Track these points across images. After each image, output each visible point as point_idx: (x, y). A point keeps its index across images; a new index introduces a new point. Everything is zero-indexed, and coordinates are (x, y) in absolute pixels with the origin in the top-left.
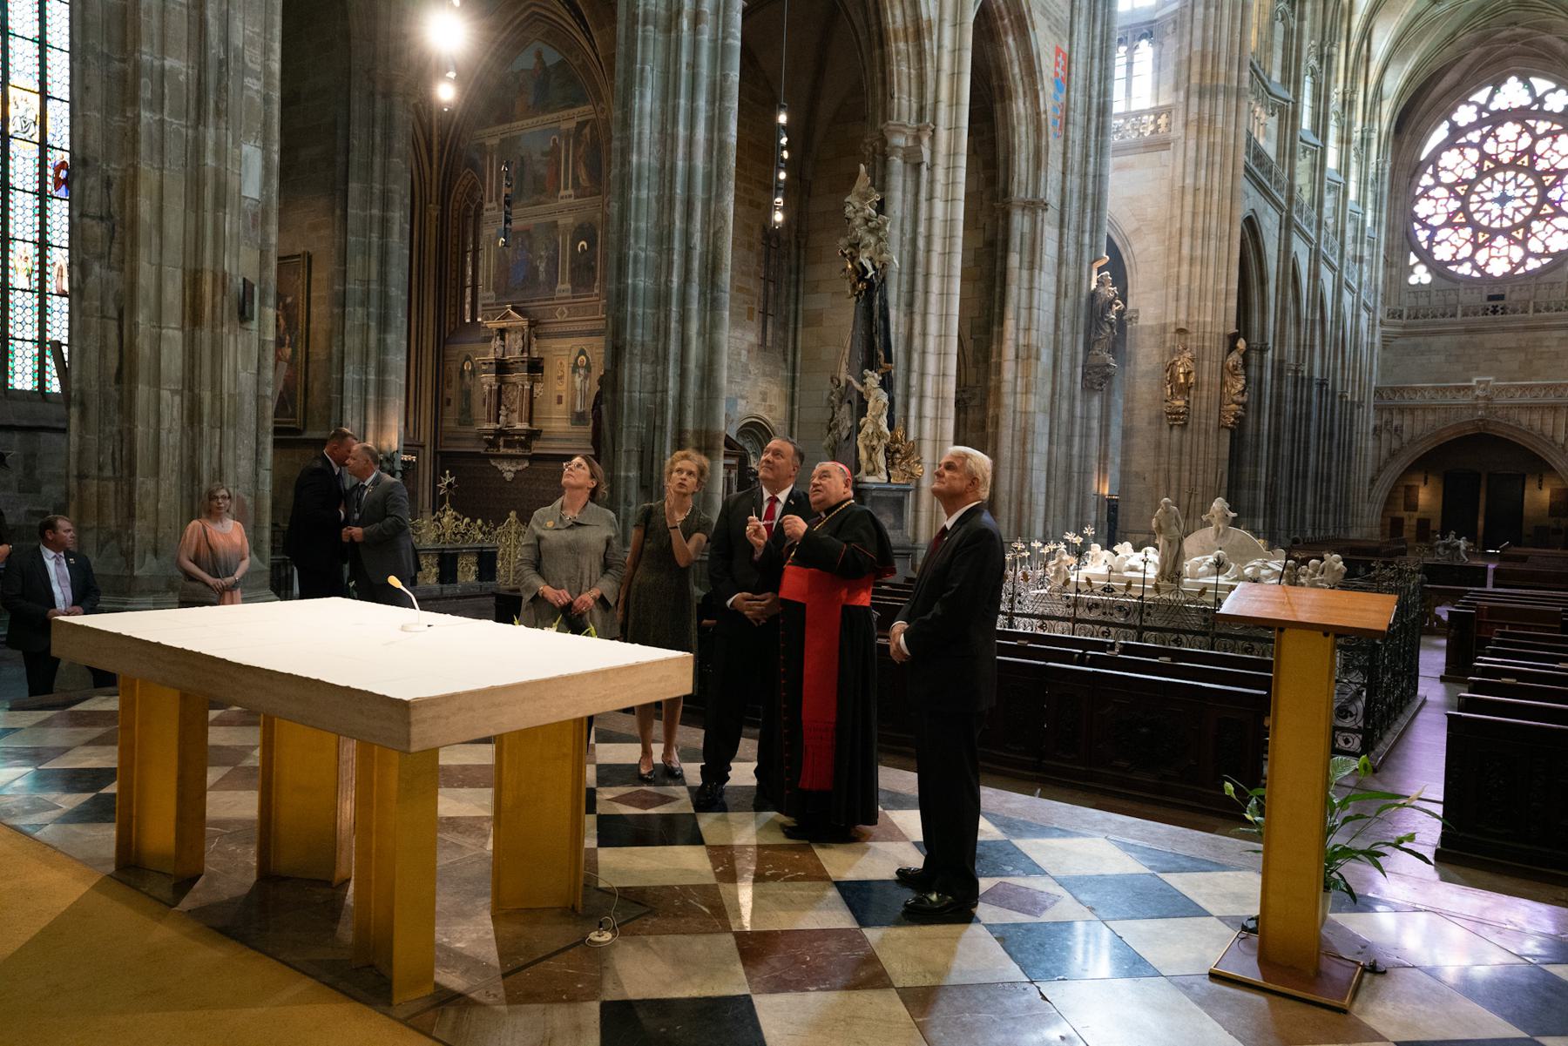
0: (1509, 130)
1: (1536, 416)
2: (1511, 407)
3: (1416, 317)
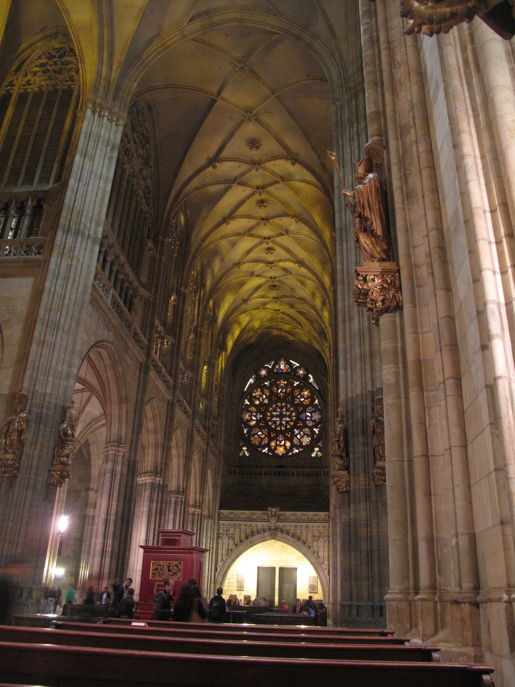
3: (242, 474)
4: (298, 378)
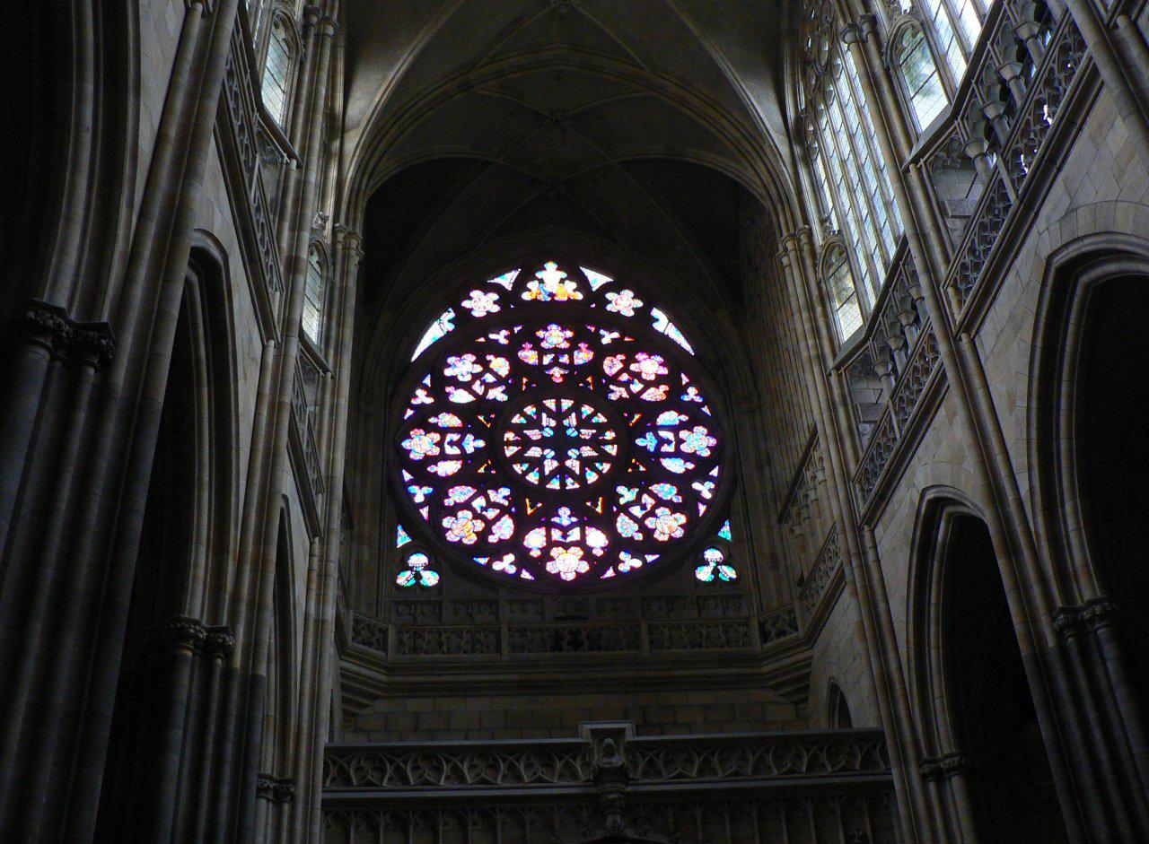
3: (415, 650)
4: (615, 321)
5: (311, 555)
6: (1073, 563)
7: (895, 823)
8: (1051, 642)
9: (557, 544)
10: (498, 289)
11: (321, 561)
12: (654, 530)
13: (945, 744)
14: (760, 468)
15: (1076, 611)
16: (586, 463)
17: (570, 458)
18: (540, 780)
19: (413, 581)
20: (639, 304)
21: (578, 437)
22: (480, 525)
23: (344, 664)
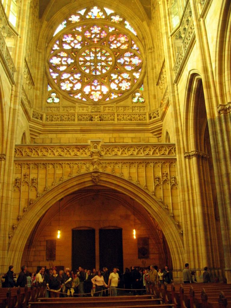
0: (96, 30)
1: (134, 170)
2: (117, 162)
3: (52, 121)
4: (114, 24)
5: (12, 90)
6: (226, 91)
7: (176, 170)
8: (216, 115)
9: (93, 91)
10: (80, 15)
11: (15, 92)
12: (121, 87)
13: (192, 148)
14: (153, 69)
15: (225, 106)
16: (103, 67)
17: (98, 66)
18: (76, 155)
19: (52, 101)
20: (121, 19)
21: (100, 60)
22: (71, 85)
23: (30, 124)
